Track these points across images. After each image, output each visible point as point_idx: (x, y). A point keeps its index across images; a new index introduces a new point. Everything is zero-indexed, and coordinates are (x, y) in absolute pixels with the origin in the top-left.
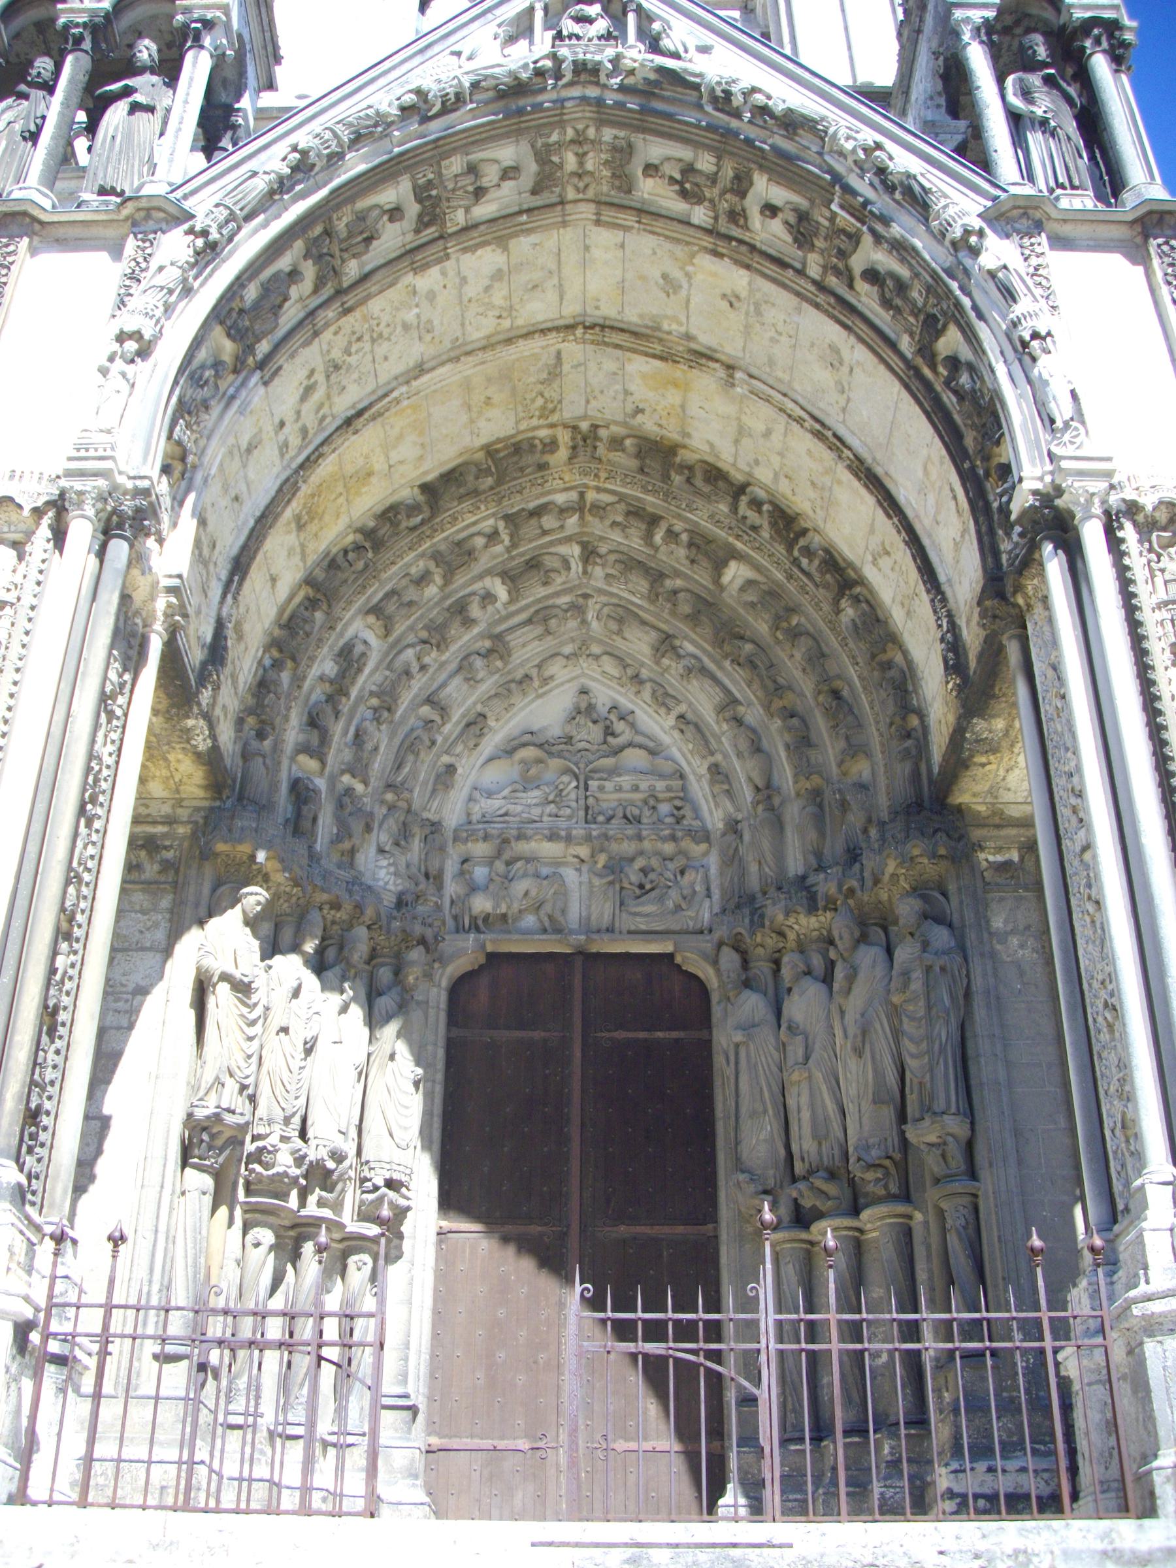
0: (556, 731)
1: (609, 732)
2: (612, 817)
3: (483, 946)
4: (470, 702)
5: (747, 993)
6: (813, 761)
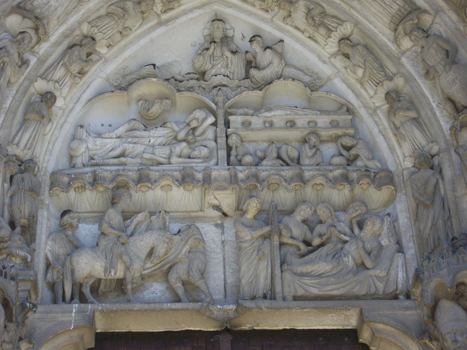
0: (183, 68)
1: (250, 64)
2: (262, 159)
3: (91, 322)
4: (73, 19)
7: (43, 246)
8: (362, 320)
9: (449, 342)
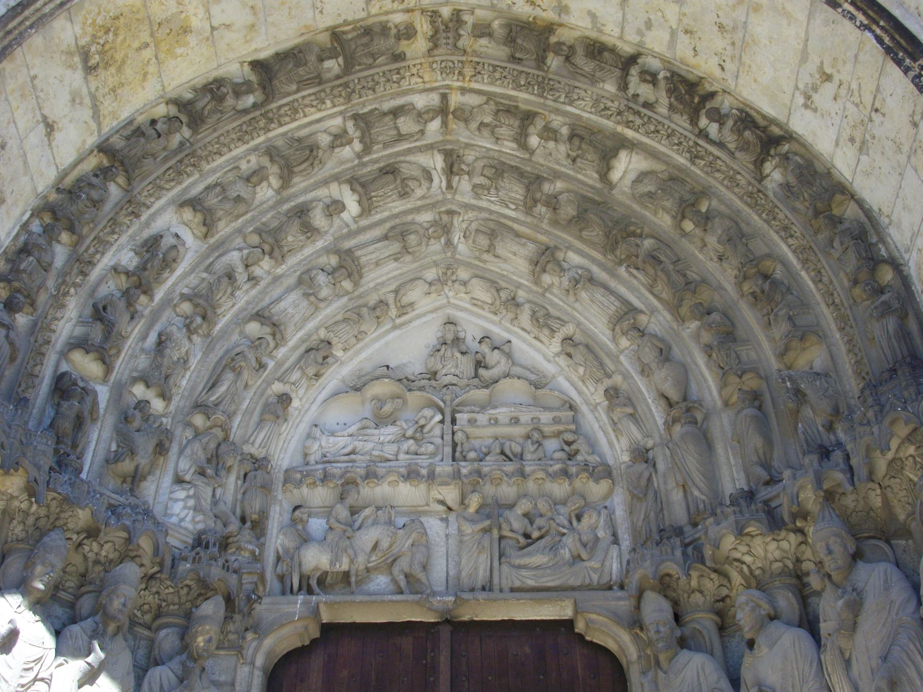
0: (416, 368)
1: (480, 364)
2: (486, 455)
3: (316, 612)
4: (310, 325)
5: (685, 655)
6: (744, 358)
7: (274, 540)
8: (576, 612)
9: (652, 632)
